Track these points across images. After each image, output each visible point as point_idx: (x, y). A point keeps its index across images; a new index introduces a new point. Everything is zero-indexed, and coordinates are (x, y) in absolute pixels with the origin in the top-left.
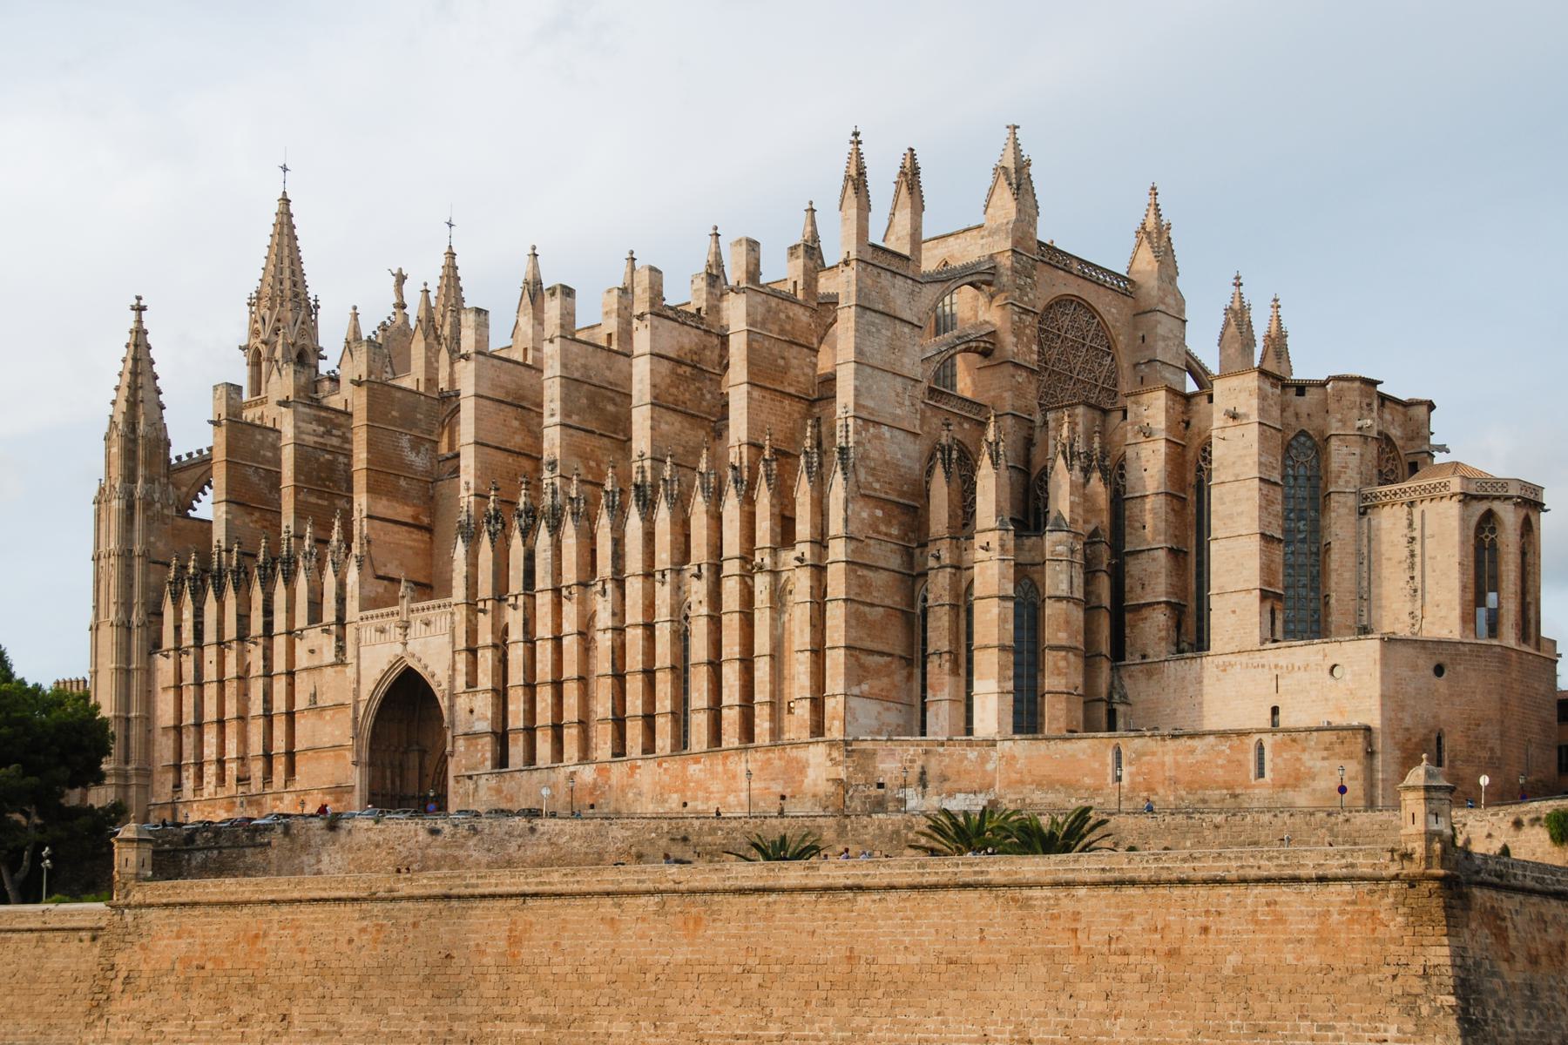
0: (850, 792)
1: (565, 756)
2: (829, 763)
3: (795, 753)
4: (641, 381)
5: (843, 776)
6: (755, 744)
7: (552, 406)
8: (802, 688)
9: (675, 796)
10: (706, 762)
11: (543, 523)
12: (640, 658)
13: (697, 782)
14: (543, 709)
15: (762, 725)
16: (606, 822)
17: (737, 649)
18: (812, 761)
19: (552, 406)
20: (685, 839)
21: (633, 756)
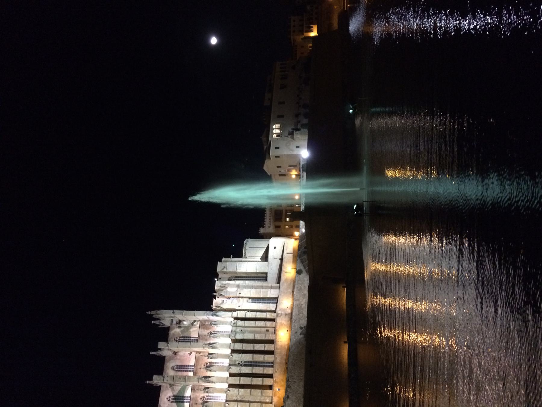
2: (281, 317)
8: (264, 324)
15: (270, 337)
17: (252, 344)
18: (280, 322)
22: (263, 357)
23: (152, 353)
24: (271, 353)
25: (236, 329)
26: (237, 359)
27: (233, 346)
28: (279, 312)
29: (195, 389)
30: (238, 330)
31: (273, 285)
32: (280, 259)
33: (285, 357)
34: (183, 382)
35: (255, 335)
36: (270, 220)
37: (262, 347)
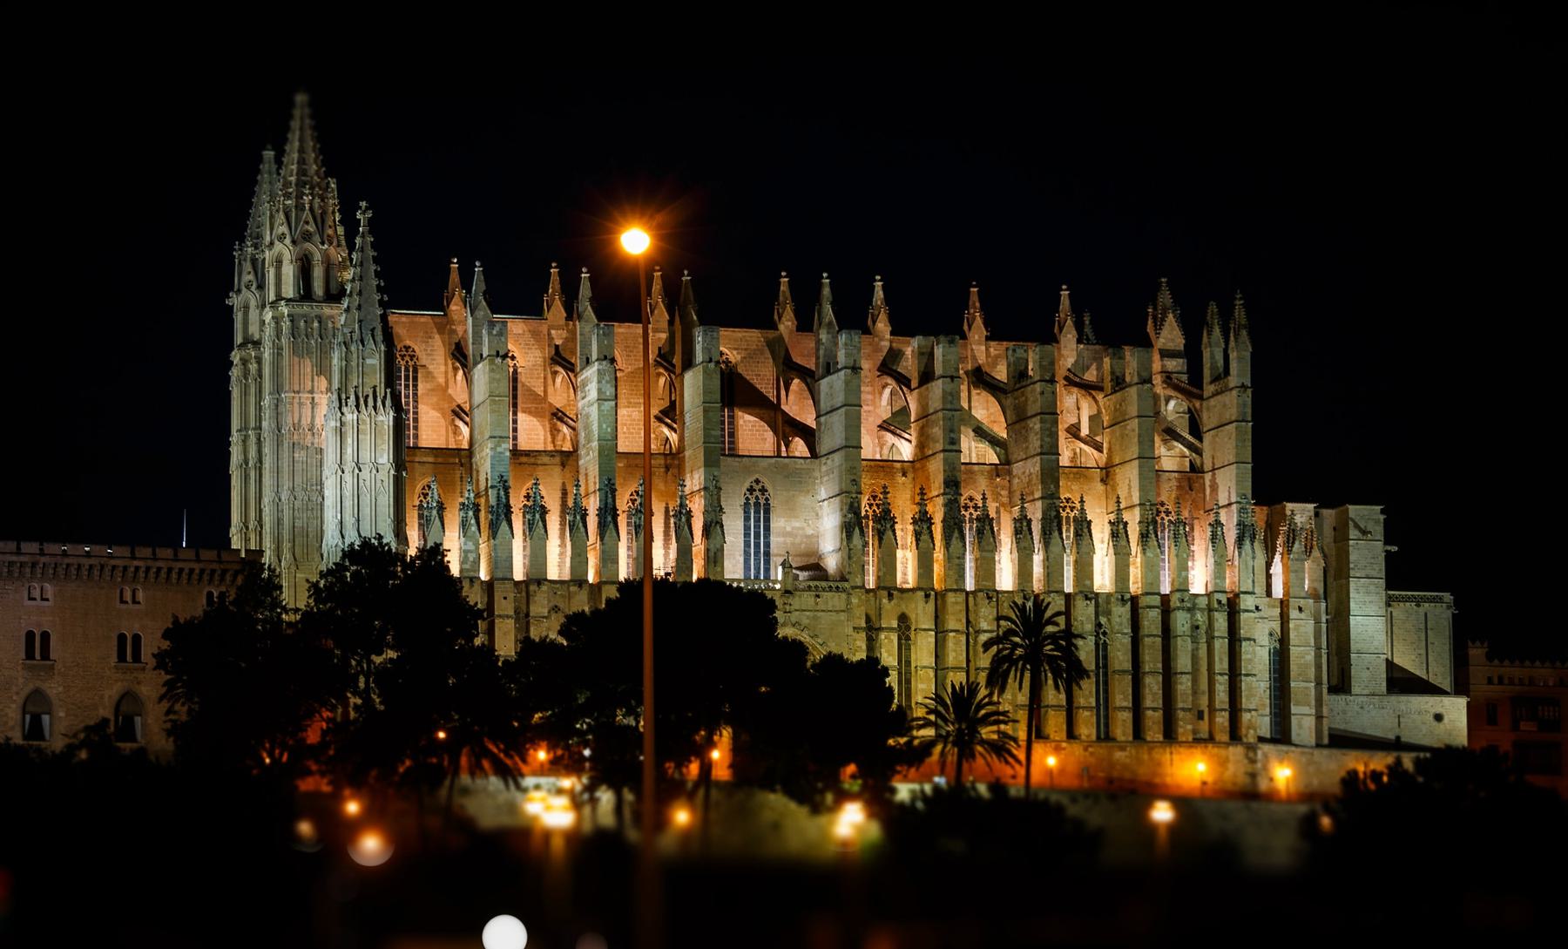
2: (1246, 761)
7: (952, 435)
8: (1222, 702)
10: (1130, 751)
15: (1185, 728)
17: (1160, 665)
18: (1231, 758)
19: (952, 435)
22: (1125, 704)
23: (1065, 293)
25: (1201, 610)
26: (1116, 620)
27: (1153, 603)
28: (1260, 753)
29: (998, 476)
30: (1201, 618)
31: (1325, 719)
32: (1398, 738)
33: (1127, 775)
34: (1042, 446)
35: (1188, 676)
36: (1516, 681)
37: (1153, 701)
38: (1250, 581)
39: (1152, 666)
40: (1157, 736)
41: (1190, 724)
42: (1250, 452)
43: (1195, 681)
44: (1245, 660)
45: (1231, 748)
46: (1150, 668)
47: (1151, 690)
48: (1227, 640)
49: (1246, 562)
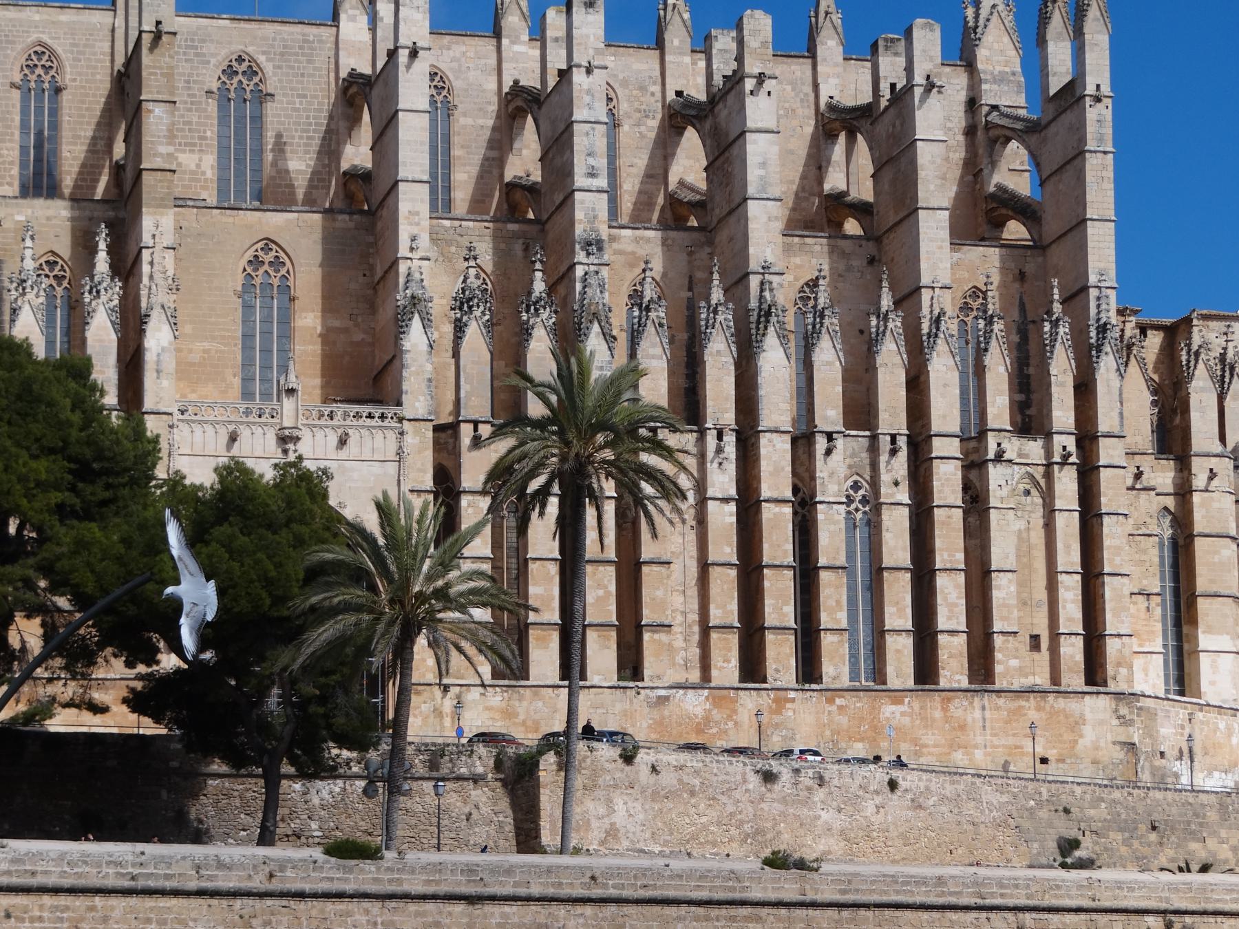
0: (1142, 762)
1: (647, 673)
2: (1115, 722)
3: (1061, 703)
4: (763, 165)
5: (1136, 740)
6: (997, 686)
7: (591, 161)
8: (1070, 620)
9: (859, 745)
10: (912, 703)
11: (596, 327)
12: (789, 547)
13: (897, 729)
14: (598, 599)
16: (978, 781)
19: (591, 161)
20: (1067, 811)
21: (778, 685)
24: (926, 671)
37: (949, 618)
38: (1115, 414)
39: (946, 556)
40: (958, 677)
41: (1016, 658)
42: (1112, 200)
43: (1024, 585)
44: (1110, 547)
45: (1087, 697)
46: (943, 560)
47: (945, 599)
48: (1077, 514)
49: (1108, 380)
